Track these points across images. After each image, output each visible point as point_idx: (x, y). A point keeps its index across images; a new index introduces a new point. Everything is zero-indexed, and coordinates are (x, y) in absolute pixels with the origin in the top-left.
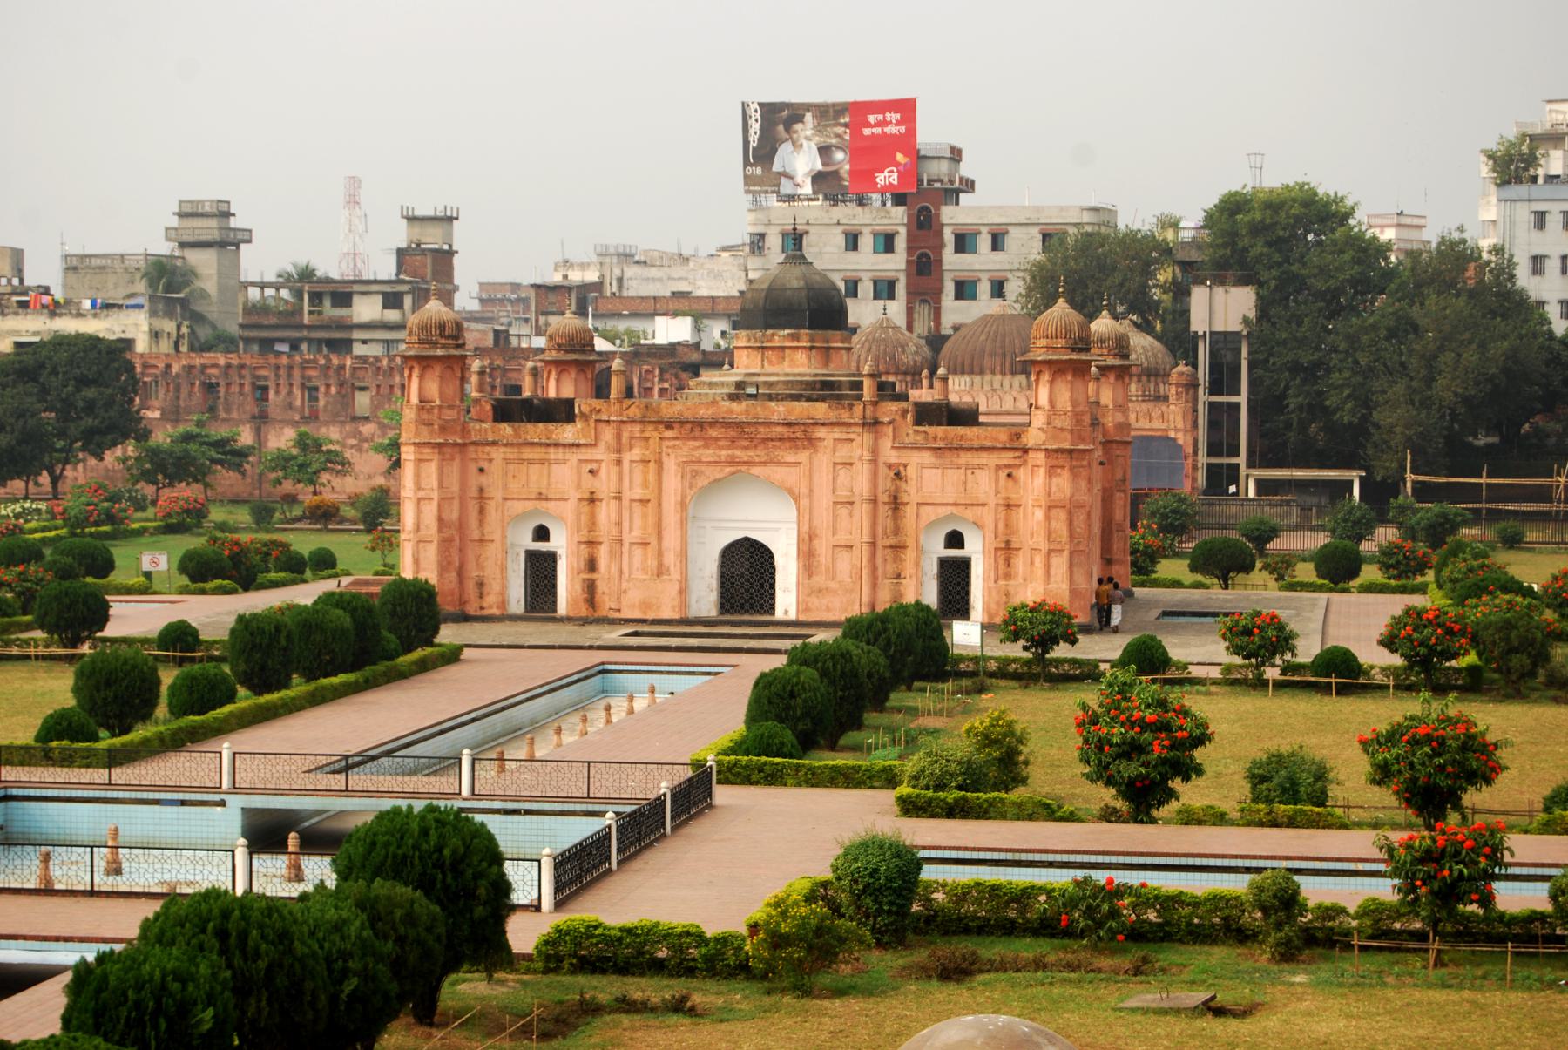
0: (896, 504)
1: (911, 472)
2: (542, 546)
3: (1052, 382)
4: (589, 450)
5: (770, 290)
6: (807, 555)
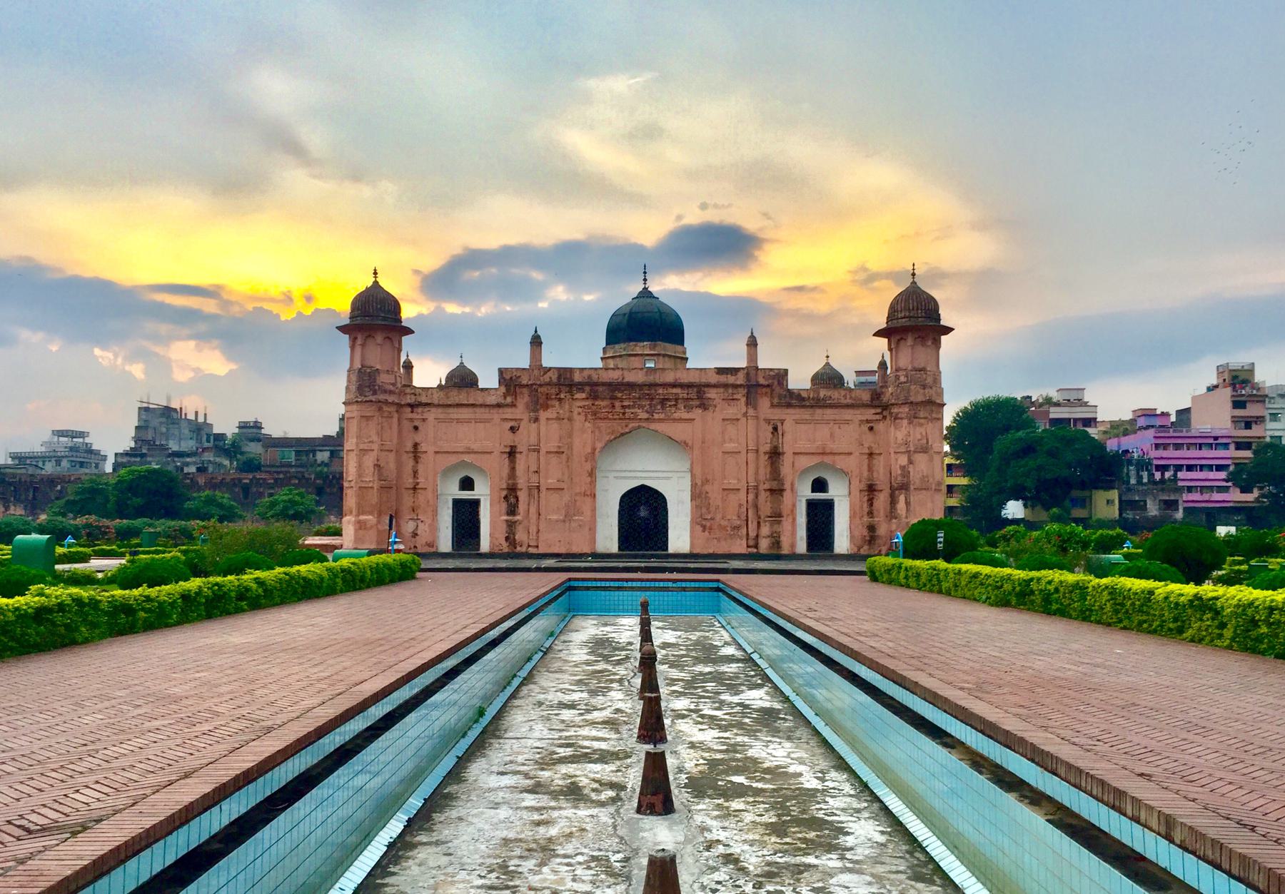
0: (775, 455)
1: (788, 426)
2: (466, 495)
3: (912, 347)
4: (509, 410)
5: (631, 313)
6: (698, 495)
